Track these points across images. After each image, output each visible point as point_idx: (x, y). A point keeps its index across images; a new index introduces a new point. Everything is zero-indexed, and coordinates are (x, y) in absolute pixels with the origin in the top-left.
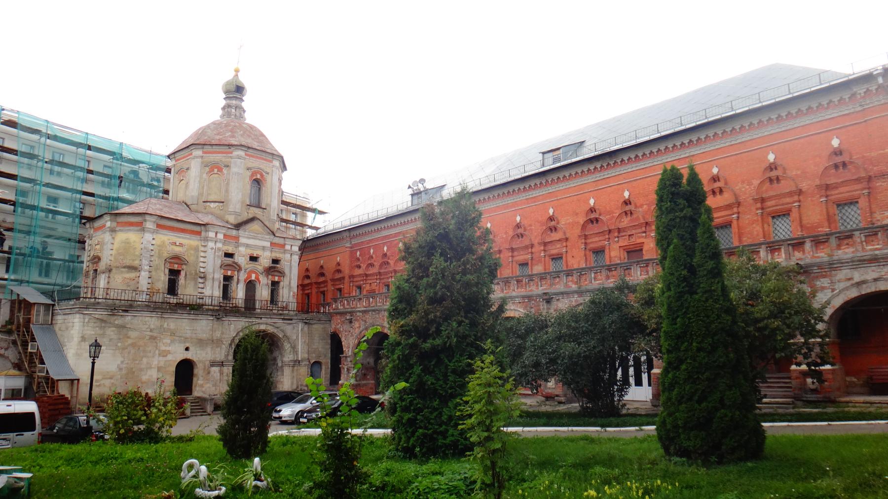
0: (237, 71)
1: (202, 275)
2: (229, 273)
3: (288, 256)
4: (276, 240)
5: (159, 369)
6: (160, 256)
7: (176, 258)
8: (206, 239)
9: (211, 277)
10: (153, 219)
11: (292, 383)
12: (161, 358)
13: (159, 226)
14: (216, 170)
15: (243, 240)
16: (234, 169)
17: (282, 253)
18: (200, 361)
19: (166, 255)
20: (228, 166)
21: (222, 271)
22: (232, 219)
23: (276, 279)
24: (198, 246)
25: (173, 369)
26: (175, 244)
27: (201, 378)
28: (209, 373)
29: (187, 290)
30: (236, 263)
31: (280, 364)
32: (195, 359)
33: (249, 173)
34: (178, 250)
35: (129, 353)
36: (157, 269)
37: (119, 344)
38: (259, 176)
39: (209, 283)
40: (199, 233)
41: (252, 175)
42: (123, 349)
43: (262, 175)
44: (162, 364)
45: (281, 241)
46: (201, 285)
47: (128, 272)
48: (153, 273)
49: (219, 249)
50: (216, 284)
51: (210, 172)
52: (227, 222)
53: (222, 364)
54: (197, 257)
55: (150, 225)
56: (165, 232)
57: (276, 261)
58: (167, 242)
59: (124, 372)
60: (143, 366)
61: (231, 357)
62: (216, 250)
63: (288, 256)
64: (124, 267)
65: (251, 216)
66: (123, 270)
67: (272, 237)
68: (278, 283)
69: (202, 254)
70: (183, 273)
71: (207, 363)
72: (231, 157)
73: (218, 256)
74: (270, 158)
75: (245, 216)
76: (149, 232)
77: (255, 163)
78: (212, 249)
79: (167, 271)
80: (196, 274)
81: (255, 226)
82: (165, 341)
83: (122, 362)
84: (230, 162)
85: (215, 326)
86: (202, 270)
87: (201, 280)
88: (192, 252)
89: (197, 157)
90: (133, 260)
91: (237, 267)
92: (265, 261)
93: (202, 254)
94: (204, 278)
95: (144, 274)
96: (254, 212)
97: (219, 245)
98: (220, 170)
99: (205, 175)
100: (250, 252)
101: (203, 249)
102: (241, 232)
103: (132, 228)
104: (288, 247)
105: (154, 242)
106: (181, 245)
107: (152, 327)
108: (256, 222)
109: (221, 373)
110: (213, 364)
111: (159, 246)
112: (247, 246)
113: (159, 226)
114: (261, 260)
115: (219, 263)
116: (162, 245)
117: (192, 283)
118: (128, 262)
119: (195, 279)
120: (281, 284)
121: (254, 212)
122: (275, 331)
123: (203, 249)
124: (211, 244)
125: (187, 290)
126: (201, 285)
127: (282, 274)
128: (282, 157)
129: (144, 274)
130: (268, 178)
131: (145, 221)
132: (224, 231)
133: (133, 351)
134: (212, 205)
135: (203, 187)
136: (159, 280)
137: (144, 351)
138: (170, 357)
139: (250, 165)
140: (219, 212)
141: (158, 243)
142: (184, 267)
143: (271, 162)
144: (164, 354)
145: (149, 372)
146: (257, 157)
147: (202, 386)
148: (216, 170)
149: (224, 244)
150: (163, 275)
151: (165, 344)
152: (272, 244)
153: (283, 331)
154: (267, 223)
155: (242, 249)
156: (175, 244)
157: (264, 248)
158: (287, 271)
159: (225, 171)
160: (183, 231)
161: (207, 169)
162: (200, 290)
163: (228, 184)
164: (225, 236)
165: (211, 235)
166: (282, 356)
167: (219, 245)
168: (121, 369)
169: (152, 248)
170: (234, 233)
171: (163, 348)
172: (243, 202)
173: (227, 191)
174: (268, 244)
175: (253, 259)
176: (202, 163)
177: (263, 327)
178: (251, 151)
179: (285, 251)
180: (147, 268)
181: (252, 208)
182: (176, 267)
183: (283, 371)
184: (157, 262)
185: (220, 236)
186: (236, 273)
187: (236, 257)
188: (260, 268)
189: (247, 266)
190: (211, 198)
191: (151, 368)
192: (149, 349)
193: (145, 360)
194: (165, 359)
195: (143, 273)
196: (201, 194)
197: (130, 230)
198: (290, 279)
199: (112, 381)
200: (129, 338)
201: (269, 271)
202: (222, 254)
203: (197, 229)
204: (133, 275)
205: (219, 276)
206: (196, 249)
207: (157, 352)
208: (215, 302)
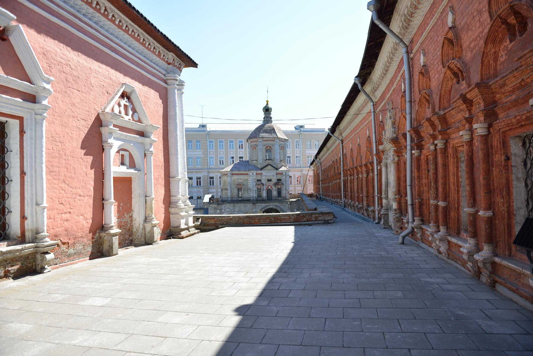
0: (267, 102)
4: (278, 172)
6: (234, 185)
16: (259, 147)
22: (259, 166)
33: (265, 147)
34: (240, 181)
41: (267, 147)
43: (270, 147)
50: (254, 192)
57: (279, 180)
68: (280, 189)
81: (269, 167)
92: (274, 180)
96: (268, 162)
97: (255, 177)
98: (255, 148)
100: (267, 178)
102: (262, 172)
118: (225, 187)
121: (268, 162)
129: (229, 191)
134: (254, 162)
155: (264, 178)
157: (273, 176)
158: (284, 183)
170: (260, 172)
175: (269, 180)
177: (271, 207)
190: (254, 159)
201: (276, 184)
204: (226, 192)
205: (255, 189)
206: (247, 180)
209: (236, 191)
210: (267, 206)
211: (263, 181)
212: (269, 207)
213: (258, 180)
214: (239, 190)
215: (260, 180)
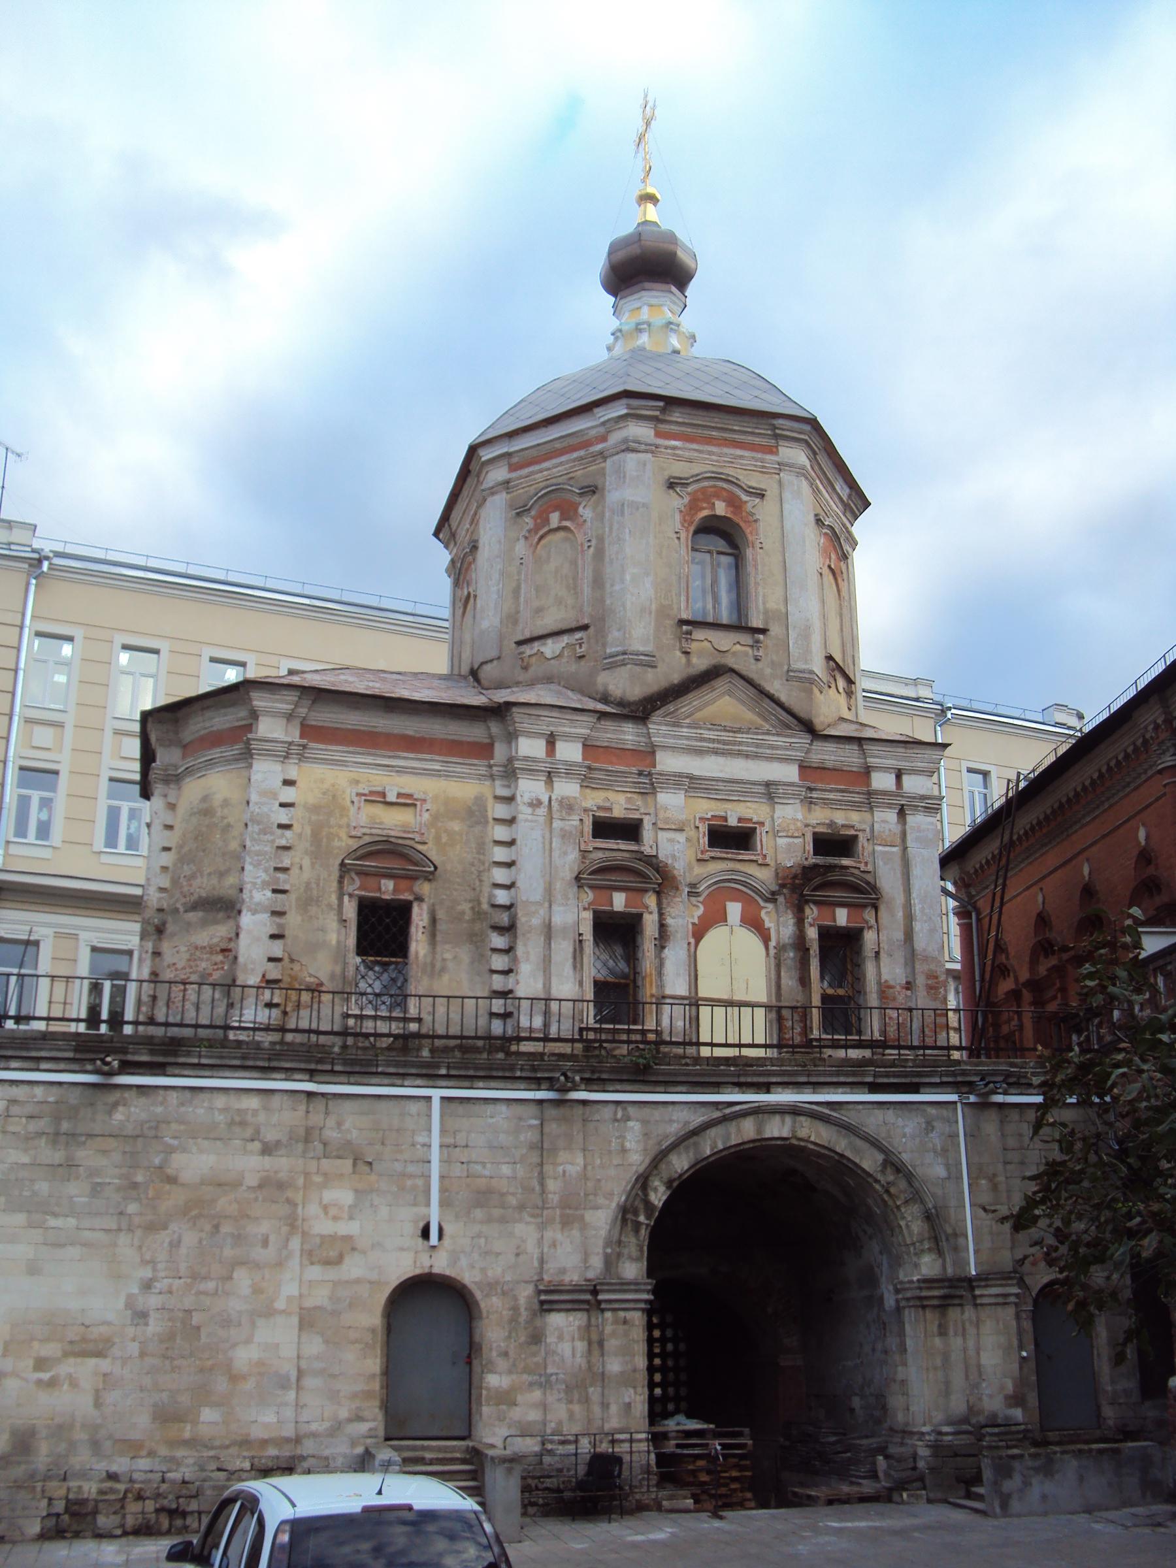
1: (504, 919)
2: (619, 901)
3: (886, 819)
4: (826, 754)
5: (307, 1321)
6: (318, 851)
7: (389, 854)
8: (510, 773)
9: (536, 921)
10: (283, 703)
11: (947, 1392)
12: (315, 1272)
13: (310, 732)
14: (555, 519)
15: (668, 762)
17: (855, 806)
18: (492, 1287)
19: (343, 844)
20: (592, 490)
21: (589, 896)
23: (842, 917)
24: (479, 801)
25: (372, 1318)
26: (378, 798)
27: (502, 1364)
28: (536, 1338)
29: (445, 982)
30: (651, 861)
31: (890, 1301)
32: (468, 1276)
33: (677, 502)
34: (393, 821)
35: (175, 1244)
36: (307, 902)
37: (132, 1208)
38: (721, 509)
39: (529, 950)
40: (484, 750)
41: (693, 506)
42: (152, 1228)
43: (734, 503)
44: (320, 1297)
45: (849, 757)
46: (499, 962)
47: (204, 923)
48: (293, 920)
49: (568, 806)
50: (563, 949)
51: (536, 529)
52: (605, 699)
53: (589, 1298)
54: (481, 848)
55: (271, 729)
56: (336, 751)
57: (835, 844)
58: (349, 793)
59: (154, 1327)
60: (235, 1305)
61: (633, 1269)
62: (551, 810)
63: (886, 819)
64: (194, 907)
65: (700, 664)
66: (193, 916)
67: (804, 739)
69: (501, 833)
70: (419, 917)
71: (525, 1293)
72: (603, 456)
73: (565, 835)
74: (760, 434)
75: (673, 668)
76: (269, 754)
77: (698, 460)
78: (535, 804)
79: (350, 910)
80: (479, 915)
81: (723, 704)
82: (329, 1195)
83: (147, 1286)
84: (602, 473)
85: (552, 1128)
86: (502, 897)
87: (498, 941)
88: (456, 826)
89: (493, 491)
90: (222, 875)
91: (655, 877)
93: (501, 833)
94: (509, 929)
95: (254, 924)
98: (569, 511)
99: (521, 548)
100: (707, 808)
101: (501, 811)
102: (659, 728)
103: (216, 753)
104: (882, 781)
105: (288, 794)
106: (407, 802)
107: (271, 1136)
108: (722, 684)
109: (596, 1344)
110: (551, 1298)
111: (315, 809)
112: (693, 784)
113: (310, 732)
114: (763, 840)
115: (568, 861)
116: (329, 806)
117: (465, 953)
118: (203, 886)
119: (475, 939)
120: (869, 937)
122: (842, 1144)
123: (501, 811)
124: (529, 788)
125: (445, 982)
126: (499, 962)
127: (866, 894)
128: (813, 423)
130: (764, 512)
131: (254, 715)
132: (582, 727)
133: (190, 1239)
134: (550, 648)
135: (516, 591)
136: (314, 947)
137: (239, 1239)
138: (353, 1268)
139: (680, 469)
140: (573, 667)
141: (311, 800)
142: (424, 888)
143: (772, 450)
144: (331, 1251)
145: (265, 1333)
146: (709, 441)
147: (506, 1398)
148: (555, 519)
149: (587, 782)
150: (332, 923)
151: (333, 1205)
152: (805, 769)
153: (875, 1144)
154: (776, 687)
155: (671, 801)
156: (378, 798)
157: (770, 791)
158: (888, 881)
159: (586, 512)
160: (414, 744)
161: (528, 522)
162: (498, 983)
163: (600, 554)
164: (589, 747)
165: (530, 747)
166: (896, 1262)
167: (567, 788)
168: (142, 1316)
169: (283, 817)
170: (628, 734)
171: (323, 1226)
172: (662, 612)
173: (598, 582)
174: (791, 773)
175: (730, 839)
176: (511, 505)
177: (777, 1129)
178: (677, 416)
179: (871, 800)
180: (263, 896)
181: (699, 634)
182: (387, 889)
183: (902, 1334)
184: (307, 874)
185: (570, 752)
186: (651, 900)
187: (647, 833)
188: (764, 877)
189: (699, 870)
190: (550, 621)
191: (269, 1312)
192: (264, 1227)
193: (243, 1280)
194: (332, 1274)
195: (246, 919)
196: (513, 619)
197: (210, 763)
198: (909, 918)
199: (105, 1365)
200: (172, 1180)
202: (579, 824)
203: (473, 732)
204: (218, 932)
205: (574, 915)
206: (475, 814)
207: (295, 1243)
208: (564, 1027)
209: (332, 937)
210: (730, 1116)
211: (675, 845)
212: (747, 1130)
213: (605, 828)
214: (382, 932)
215: (629, 830)
